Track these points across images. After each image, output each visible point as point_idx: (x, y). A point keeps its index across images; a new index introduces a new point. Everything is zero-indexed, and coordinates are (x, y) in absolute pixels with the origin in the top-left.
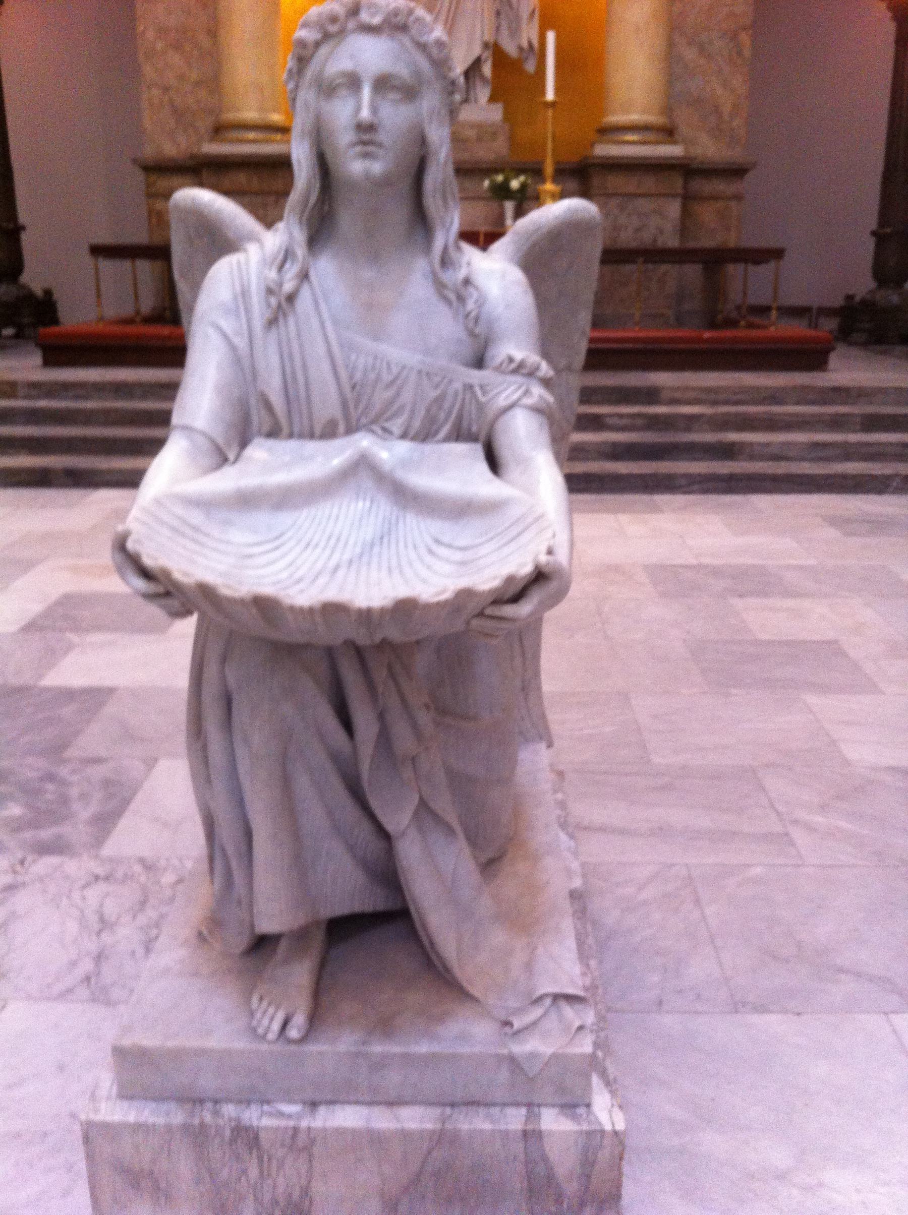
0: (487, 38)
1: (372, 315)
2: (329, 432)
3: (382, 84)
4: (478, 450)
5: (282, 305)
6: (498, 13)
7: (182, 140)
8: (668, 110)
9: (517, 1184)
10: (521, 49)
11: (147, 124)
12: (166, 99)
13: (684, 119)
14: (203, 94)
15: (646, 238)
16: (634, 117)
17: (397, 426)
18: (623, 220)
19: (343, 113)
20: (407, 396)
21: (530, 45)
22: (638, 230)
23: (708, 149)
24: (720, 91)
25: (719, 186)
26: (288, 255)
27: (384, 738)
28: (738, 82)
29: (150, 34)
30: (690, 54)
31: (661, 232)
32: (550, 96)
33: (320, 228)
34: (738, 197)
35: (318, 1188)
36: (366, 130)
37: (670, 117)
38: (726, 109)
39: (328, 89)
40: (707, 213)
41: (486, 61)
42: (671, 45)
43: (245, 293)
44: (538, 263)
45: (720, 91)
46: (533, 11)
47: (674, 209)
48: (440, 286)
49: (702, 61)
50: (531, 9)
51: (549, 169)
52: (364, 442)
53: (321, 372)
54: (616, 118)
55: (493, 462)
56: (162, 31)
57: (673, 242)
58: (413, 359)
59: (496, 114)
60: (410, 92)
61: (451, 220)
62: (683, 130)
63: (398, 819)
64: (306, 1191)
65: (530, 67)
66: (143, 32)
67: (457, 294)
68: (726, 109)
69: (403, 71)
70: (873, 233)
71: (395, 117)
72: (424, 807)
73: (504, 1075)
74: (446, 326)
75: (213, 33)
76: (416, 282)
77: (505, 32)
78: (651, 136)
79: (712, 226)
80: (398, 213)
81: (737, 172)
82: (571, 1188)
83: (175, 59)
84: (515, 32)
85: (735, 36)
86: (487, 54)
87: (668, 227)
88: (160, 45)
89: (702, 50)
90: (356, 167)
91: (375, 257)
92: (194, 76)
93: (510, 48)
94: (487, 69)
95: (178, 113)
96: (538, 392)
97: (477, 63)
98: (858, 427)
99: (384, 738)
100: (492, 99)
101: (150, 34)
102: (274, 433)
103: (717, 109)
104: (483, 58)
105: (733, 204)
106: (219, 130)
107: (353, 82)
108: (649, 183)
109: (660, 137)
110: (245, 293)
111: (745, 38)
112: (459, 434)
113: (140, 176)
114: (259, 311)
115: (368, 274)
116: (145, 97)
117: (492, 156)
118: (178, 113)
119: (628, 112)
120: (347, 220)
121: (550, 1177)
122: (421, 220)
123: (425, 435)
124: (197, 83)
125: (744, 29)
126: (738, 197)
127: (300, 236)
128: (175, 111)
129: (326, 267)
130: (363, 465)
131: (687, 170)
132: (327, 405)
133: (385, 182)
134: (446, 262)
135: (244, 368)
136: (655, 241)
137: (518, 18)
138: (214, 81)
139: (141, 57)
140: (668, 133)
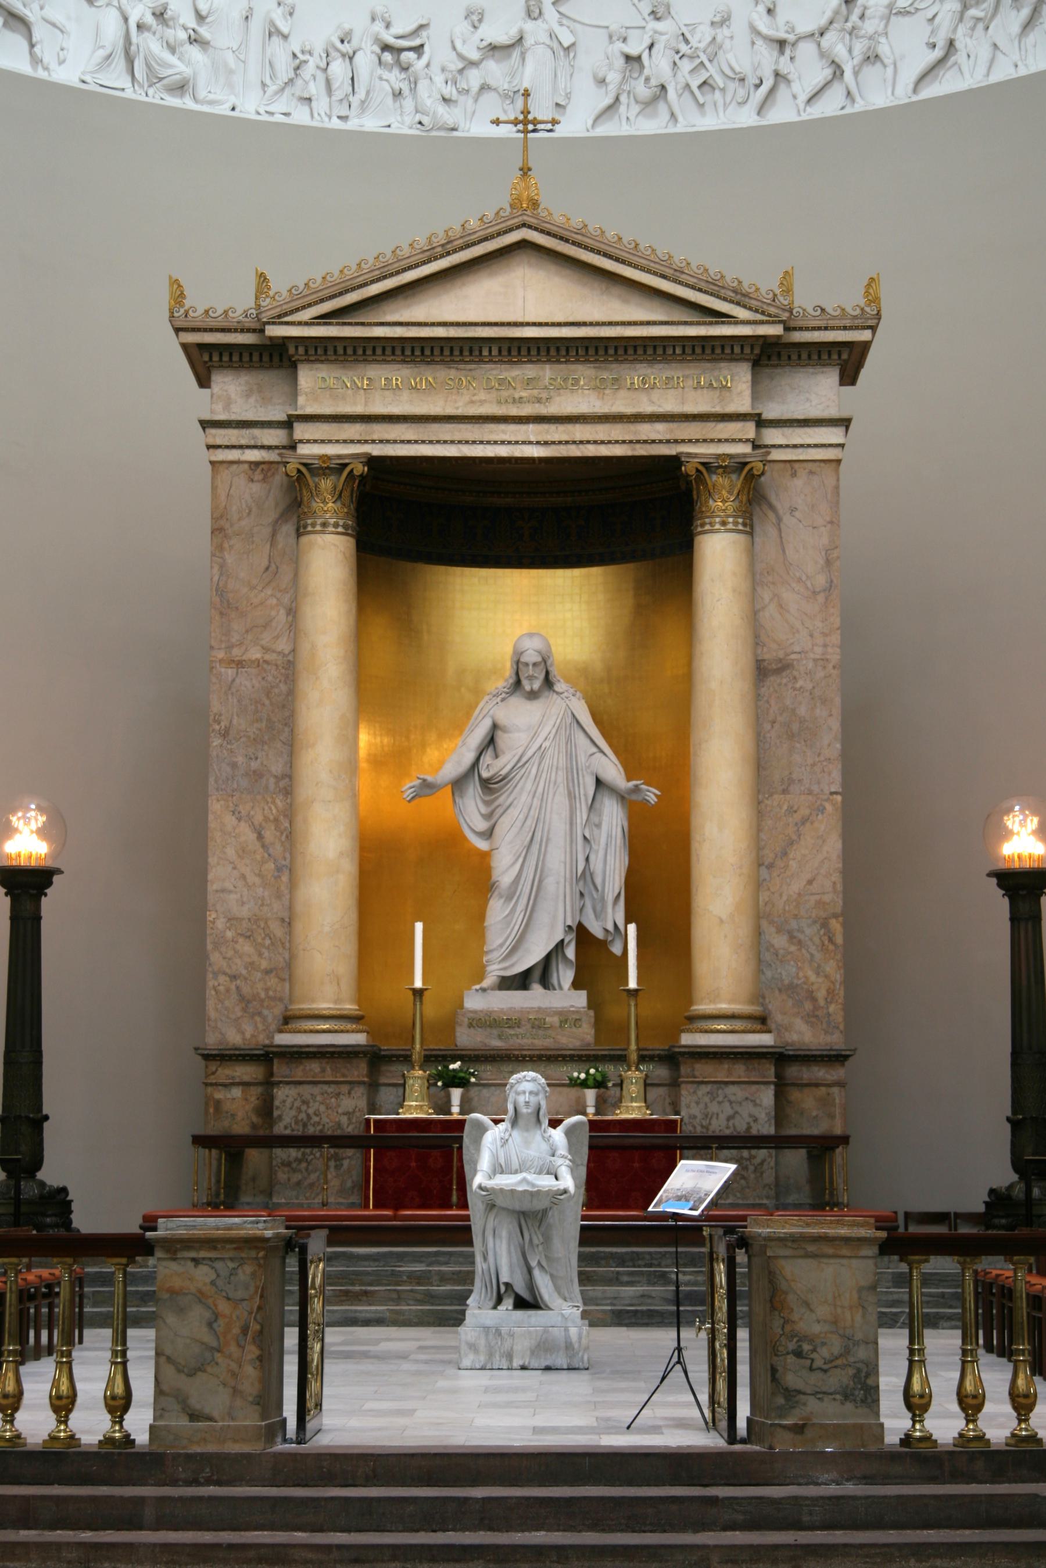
0: (569, 923)
1: (527, 1143)
2: (516, 1172)
3: (531, 1093)
4: (553, 1177)
5: (505, 1142)
6: (582, 894)
7: (249, 1030)
8: (758, 997)
9: (563, 1345)
10: (606, 931)
11: (212, 1014)
12: (233, 987)
13: (777, 1006)
14: (272, 981)
15: (740, 1126)
16: (724, 1007)
17: (532, 1171)
18: (714, 1108)
19: (521, 1099)
20: (535, 1163)
21: (616, 926)
22: (729, 1119)
23: (803, 1035)
24: (813, 978)
25: (820, 1073)
26: (506, 1130)
27: (531, 1240)
28: (831, 967)
29: (220, 924)
30: (780, 941)
31: (756, 1120)
32: (632, 984)
33: (514, 1123)
34: (840, 1084)
35: (515, 1347)
36: (527, 1103)
37: (763, 1005)
38: (821, 995)
39: (518, 1094)
40: (806, 1101)
41: (570, 942)
42: (758, 933)
43: (495, 1139)
44: (569, 1133)
45: (813, 978)
46: (619, 894)
47: (767, 1097)
48: (543, 1137)
49: (793, 948)
50: (616, 894)
51: (634, 1057)
52: (524, 1175)
53: (514, 1158)
54: (702, 1007)
55: (557, 1178)
56: (232, 920)
57: (769, 1130)
58: (537, 1155)
59: (579, 999)
60: (537, 1094)
61: (545, 1123)
62: (777, 1018)
63: (533, 1263)
64: (512, 1348)
65: (616, 949)
66: (214, 923)
67: (547, 1139)
68: (821, 995)
69: (535, 1090)
70: (1008, 1119)
71: (533, 1100)
72: (539, 1263)
73: (560, 1318)
74: (544, 1147)
75: (288, 922)
76: (538, 1137)
77: (589, 910)
78: (738, 1025)
79: (814, 1114)
80: (534, 1119)
81: (838, 1058)
82: (576, 1346)
83: (246, 947)
84: (598, 915)
85: (825, 924)
86: (571, 939)
87: (762, 1116)
88: (229, 934)
89: (792, 937)
90: (524, 1110)
91: (527, 1130)
92: (264, 964)
93: (596, 929)
94: (570, 952)
95: (244, 1001)
96: (568, 1162)
97: (560, 945)
98: (890, 1284)
99: (531, 1240)
100: (576, 985)
101: (220, 924)
102: (502, 1173)
103: (812, 997)
104: (566, 942)
105: (835, 1090)
106: (287, 1020)
107: (524, 1092)
108: (739, 1071)
109: (748, 1025)
110: (495, 1139)
111: (836, 925)
112: (548, 1173)
113: (203, 1062)
114: (499, 1144)
115: (526, 1134)
116: (211, 983)
117: (577, 1044)
118: (244, 1001)
119: (713, 1001)
120: (521, 1122)
121: (571, 1343)
122: (538, 1121)
123: (540, 1173)
124: (267, 972)
125: (835, 916)
126: (840, 1084)
127: (509, 1126)
128: (242, 998)
129: (515, 1133)
130: (524, 1180)
131: (781, 1058)
132: (515, 1165)
133: (529, 1114)
134: (545, 1131)
135: (495, 1157)
136: (749, 1128)
137: (603, 899)
138: (286, 970)
139: (209, 947)
140: (761, 1021)
